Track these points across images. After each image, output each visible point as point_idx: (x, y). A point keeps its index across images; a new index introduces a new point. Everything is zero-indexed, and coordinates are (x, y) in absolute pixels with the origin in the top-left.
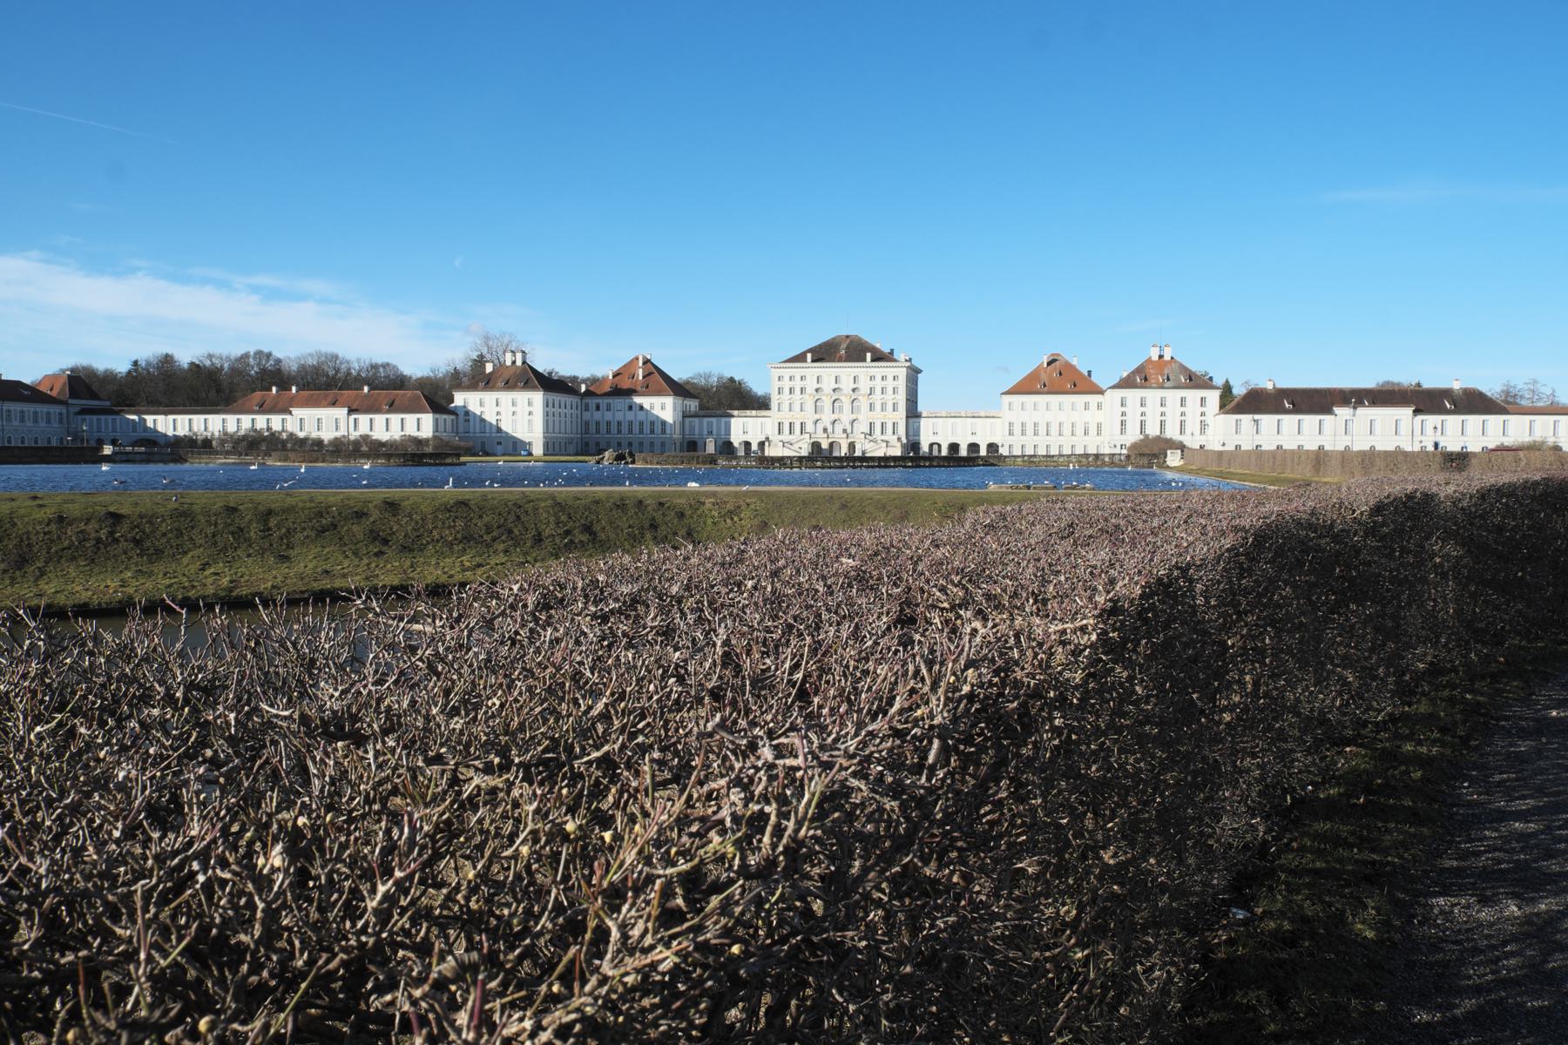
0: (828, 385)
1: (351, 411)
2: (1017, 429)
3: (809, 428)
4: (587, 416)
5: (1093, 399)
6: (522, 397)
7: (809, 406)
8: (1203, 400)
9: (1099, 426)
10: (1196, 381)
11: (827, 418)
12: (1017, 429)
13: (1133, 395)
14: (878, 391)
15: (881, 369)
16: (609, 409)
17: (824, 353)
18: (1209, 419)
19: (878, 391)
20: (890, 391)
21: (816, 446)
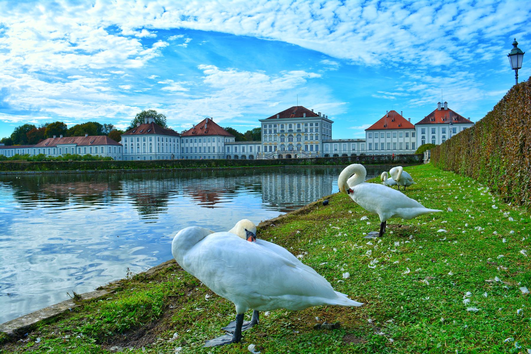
0: (286, 128)
3: (279, 148)
4: (183, 145)
5: (410, 132)
13: (428, 129)
14: (309, 131)
15: (309, 121)
16: (191, 142)
19: (309, 131)
20: (314, 130)
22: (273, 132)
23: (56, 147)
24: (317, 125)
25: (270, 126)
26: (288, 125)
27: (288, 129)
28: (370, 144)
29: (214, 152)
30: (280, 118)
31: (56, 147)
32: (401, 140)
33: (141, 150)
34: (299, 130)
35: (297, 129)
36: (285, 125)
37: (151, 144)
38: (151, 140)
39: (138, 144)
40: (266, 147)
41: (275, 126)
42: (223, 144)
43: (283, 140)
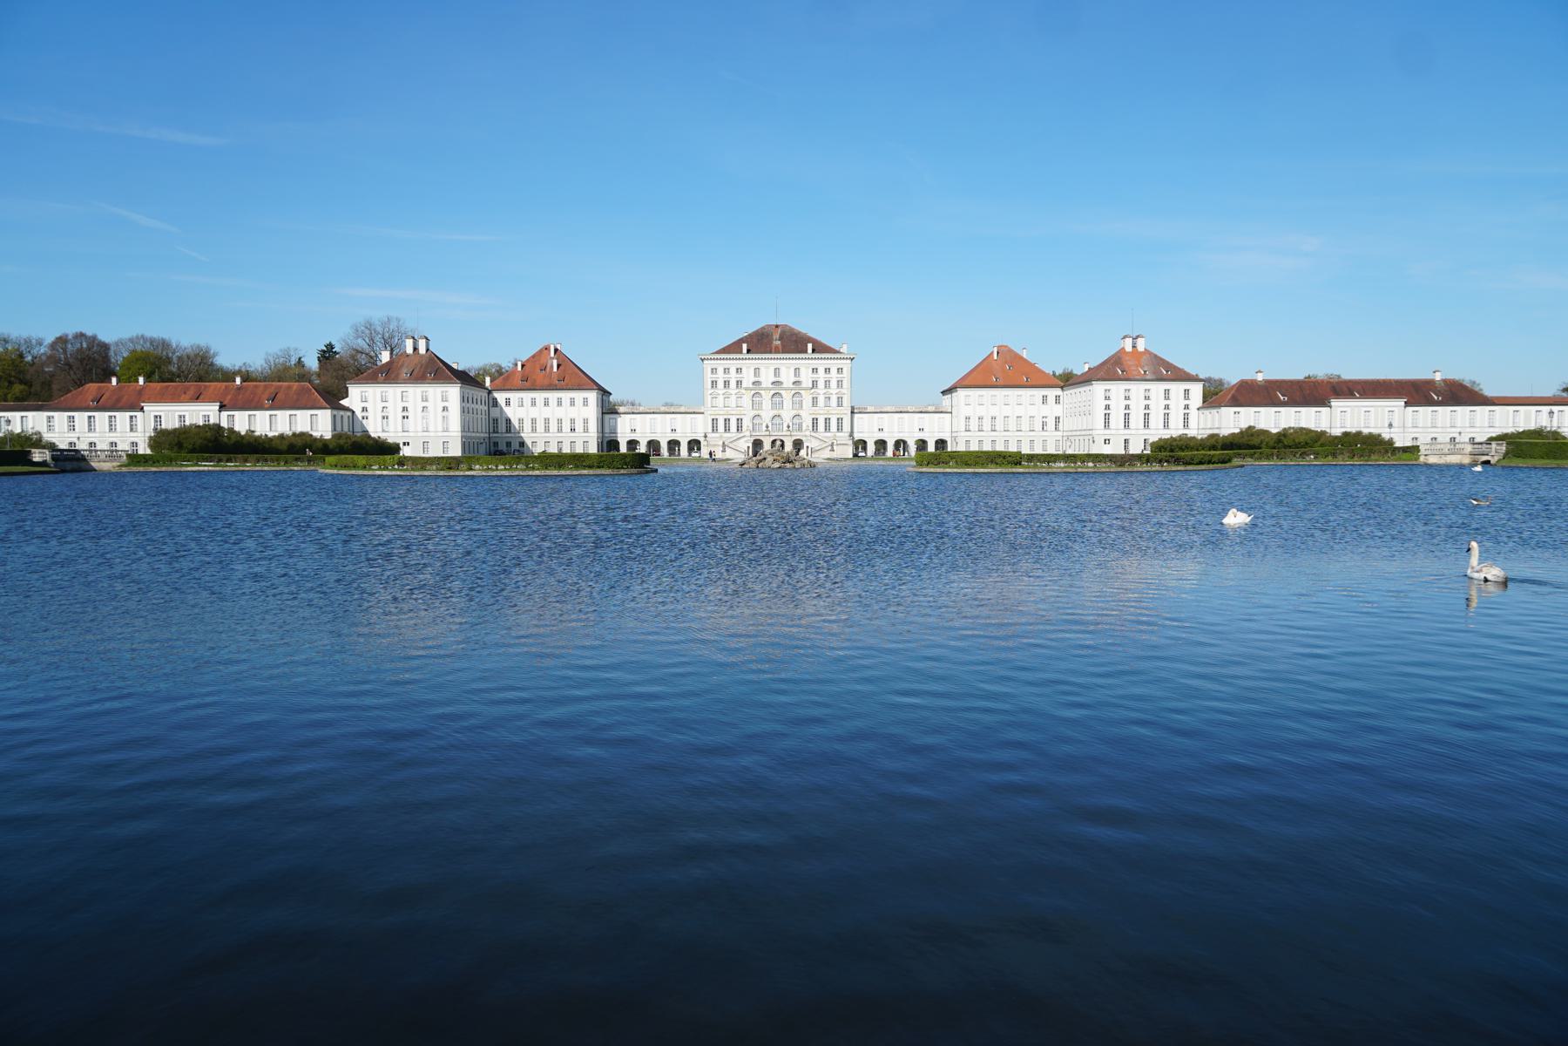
0: (767, 378)
1: (222, 407)
2: (974, 425)
3: (746, 423)
6: (435, 391)
7: (746, 400)
8: (1187, 391)
9: (1057, 419)
10: (1181, 376)
11: (767, 414)
12: (974, 425)
13: (1117, 388)
14: (821, 384)
15: (821, 362)
17: (760, 342)
18: (1193, 413)
19: (821, 384)
20: (834, 384)
21: (757, 444)
22: (733, 384)
23: (142, 409)
24: (840, 370)
25: (726, 371)
28: (968, 418)
29: (586, 430)
30: (749, 351)
31: (142, 409)
32: (1033, 411)
36: (763, 371)
38: (444, 399)
39: (405, 409)
41: (739, 370)
43: (755, 405)
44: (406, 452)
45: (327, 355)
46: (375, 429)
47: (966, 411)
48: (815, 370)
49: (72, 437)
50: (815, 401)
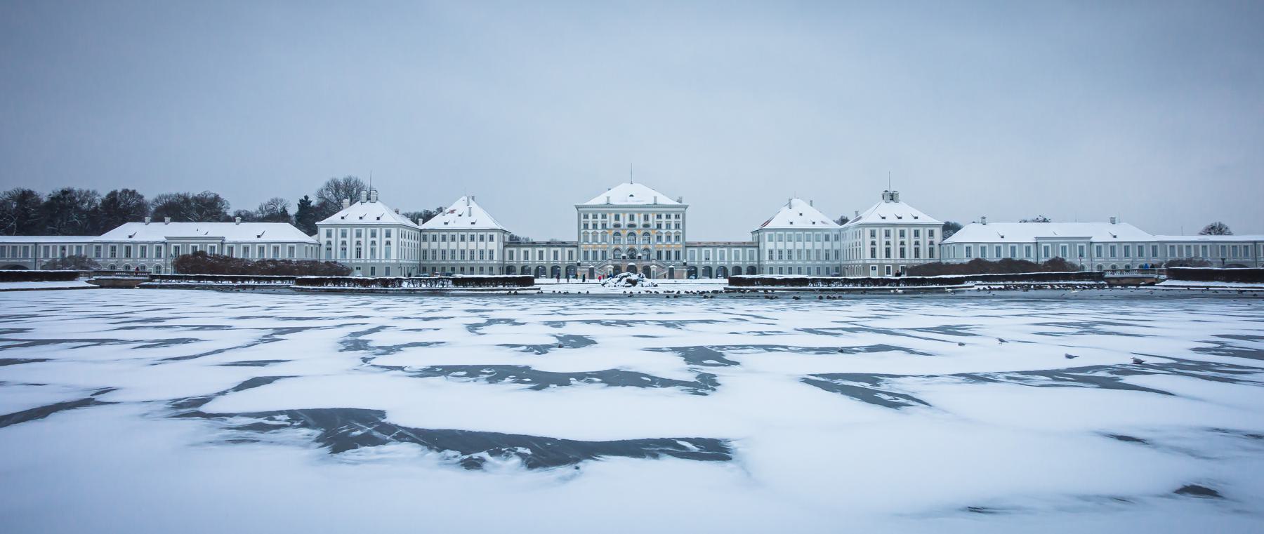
4: (425, 245)
7: (609, 237)
9: (837, 252)
19: (664, 226)
20: (673, 226)
22: (599, 226)
24: (677, 217)
26: (627, 216)
27: (628, 222)
28: (771, 252)
29: (491, 258)
33: (366, 256)
34: (646, 226)
35: (642, 222)
37: (388, 243)
40: (586, 253)
41: (604, 216)
42: (501, 245)
44: (358, 275)
45: (304, 204)
46: (336, 256)
47: (770, 245)
48: (659, 217)
49: (113, 261)
50: (659, 238)
